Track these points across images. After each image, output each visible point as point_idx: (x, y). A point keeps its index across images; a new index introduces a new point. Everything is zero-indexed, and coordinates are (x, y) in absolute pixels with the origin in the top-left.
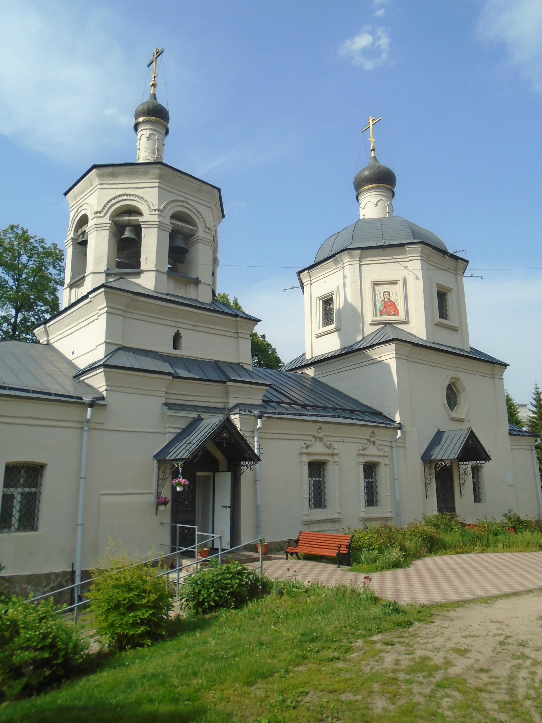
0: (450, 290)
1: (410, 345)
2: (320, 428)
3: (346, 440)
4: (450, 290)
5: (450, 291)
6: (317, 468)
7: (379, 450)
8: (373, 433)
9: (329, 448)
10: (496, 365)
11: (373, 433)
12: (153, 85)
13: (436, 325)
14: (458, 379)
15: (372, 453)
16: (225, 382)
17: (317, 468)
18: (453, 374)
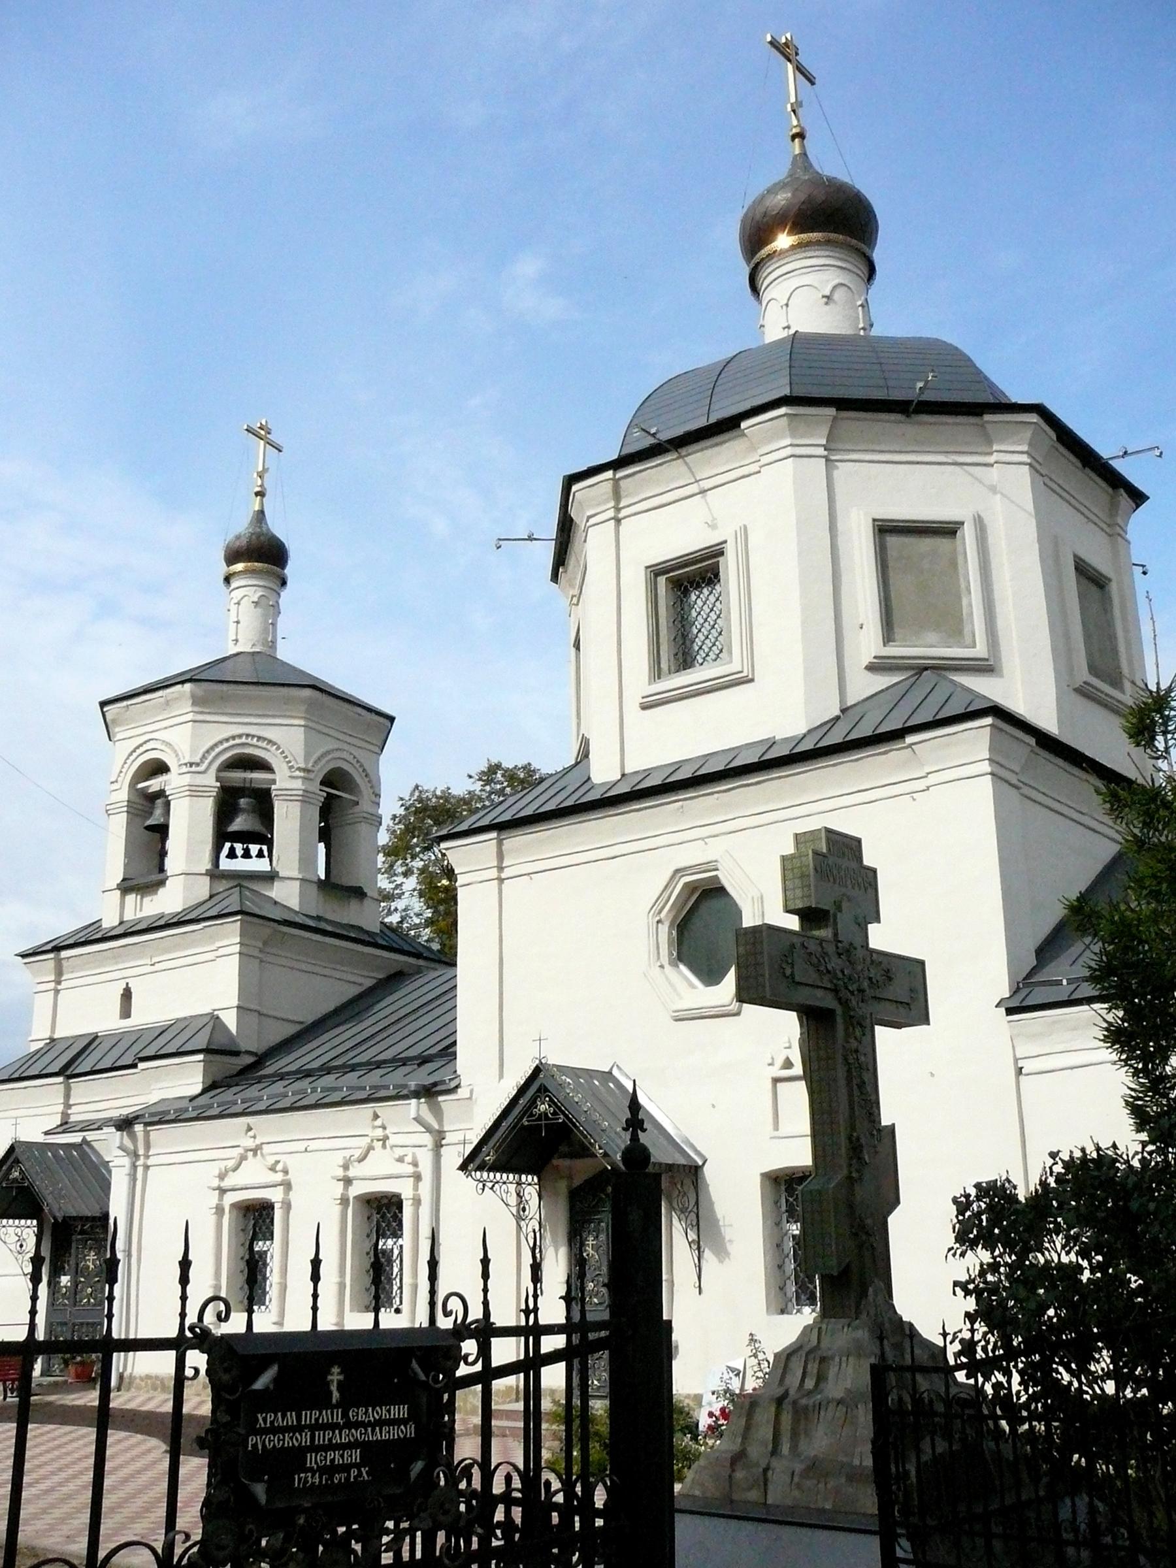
0: (717, 552)
2: (250, 1129)
3: (313, 1145)
4: (717, 552)
5: (722, 553)
6: (256, 1218)
7: (401, 1160)
8: (376, 1116)
9: (273, 1169)
10: (909, 739)
12: (260, 494)
13: (645, 707)
14: (712, 866)
15: (380, 1174)
16: (134, 1066)
18: (691, 855)
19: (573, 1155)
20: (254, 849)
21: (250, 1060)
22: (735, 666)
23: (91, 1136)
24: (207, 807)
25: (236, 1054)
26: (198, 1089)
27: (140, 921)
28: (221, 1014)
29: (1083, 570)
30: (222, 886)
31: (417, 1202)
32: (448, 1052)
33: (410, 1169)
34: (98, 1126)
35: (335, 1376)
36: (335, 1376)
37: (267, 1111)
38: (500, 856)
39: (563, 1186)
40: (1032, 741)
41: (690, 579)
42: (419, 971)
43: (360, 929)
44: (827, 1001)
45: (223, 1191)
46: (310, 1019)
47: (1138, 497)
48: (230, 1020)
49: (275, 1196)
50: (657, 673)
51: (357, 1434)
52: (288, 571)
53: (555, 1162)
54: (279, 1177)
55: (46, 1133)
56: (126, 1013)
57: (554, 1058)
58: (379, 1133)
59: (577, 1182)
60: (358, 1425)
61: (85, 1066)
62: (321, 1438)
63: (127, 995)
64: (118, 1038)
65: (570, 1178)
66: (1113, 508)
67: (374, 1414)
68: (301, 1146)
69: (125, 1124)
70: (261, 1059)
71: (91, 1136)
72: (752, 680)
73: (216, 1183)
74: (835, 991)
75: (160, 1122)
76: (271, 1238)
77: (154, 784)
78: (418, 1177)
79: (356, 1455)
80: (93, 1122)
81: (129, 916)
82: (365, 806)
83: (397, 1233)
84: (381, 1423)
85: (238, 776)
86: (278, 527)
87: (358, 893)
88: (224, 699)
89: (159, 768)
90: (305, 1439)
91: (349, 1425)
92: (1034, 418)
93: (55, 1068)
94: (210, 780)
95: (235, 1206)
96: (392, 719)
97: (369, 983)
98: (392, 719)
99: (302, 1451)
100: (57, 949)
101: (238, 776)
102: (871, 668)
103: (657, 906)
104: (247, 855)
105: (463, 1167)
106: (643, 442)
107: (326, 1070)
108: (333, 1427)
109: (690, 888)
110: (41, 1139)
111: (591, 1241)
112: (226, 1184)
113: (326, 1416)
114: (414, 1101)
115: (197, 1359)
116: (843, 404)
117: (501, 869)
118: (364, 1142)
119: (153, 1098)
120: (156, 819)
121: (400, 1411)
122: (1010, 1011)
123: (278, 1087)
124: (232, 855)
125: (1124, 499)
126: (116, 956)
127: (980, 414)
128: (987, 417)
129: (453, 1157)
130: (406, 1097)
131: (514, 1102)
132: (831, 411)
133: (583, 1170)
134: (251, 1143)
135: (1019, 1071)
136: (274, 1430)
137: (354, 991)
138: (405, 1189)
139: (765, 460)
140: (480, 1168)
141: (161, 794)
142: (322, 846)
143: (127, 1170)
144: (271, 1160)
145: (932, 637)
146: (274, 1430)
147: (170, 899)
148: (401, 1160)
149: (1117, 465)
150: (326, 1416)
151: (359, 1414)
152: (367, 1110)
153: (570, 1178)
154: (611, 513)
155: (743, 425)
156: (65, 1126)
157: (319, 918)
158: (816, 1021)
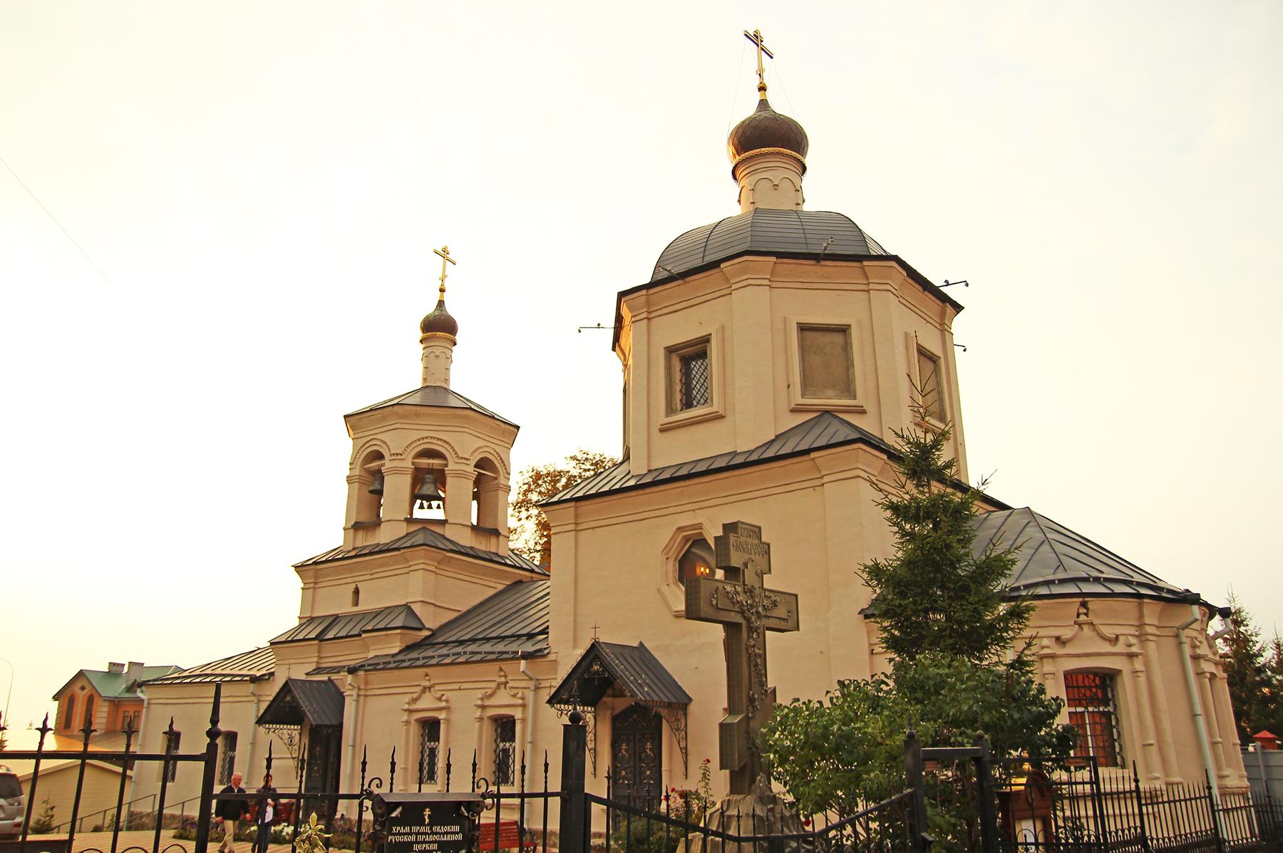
0: (706, 340)
1: (572, 504)
3: (464, 686)
4: (706, 340)
6: (431, 728)
7: (514, 696)
9: (440, 699)
10: (813, 455)
11: (501, 670)
13: (662, 431)
14: (699, 526)
15: (503, 702)
17: (431, 728)
19: (614, 696)
20: (435, 504)
21: (428, 633)
22: (714, 409)
23: (334, 677)
24: (407, 481)
25: (420, 629)
26: (396, 650)
27: (365, 547)
28: (412, 606)
29: (922, 352)
30: (414, 528)
31: (524, 720)
32: (545, 631)
33: (520, 702)
34: (337, 670)
35: (427, 812)
36: (427, 812)
37: (437, 665)
38: (577, 516)
39: (608, 714)
40: (885, 457)
41: (691, 355)
42: (533, 581)
43: (497, 554)
44: (738, 619)
45: (410, 711)
46: (464, 609)
47: (958, 308)
48: (417, 609)
49: (442, 716)
50: (670, 410)
51: (436, 837)
52: (458, 337)
53: (604, 699)
54: (443, 704)
55: (307, 674)
56: (356, 603)
57: (603, 639)
58: (503, 679)
59: (617, 711)
60: (436, 833)
61: (330, 635)
62: (420, 838)
63: (357, 592)
64: (350, 617)
65: (613, 709)
66: (943, 314)
67: (444, 829)
68: (456, 686)
69: (352, 671)
70: (434, 633)
71: (334, 677)
72: (723, 417)
73: (406, 707)
74: (742, 613)
75: (374, 670)
76: (438, 740)
77: (374, 464)
78: (524, 706)
79: (436, 846)
80: (334, 668)
81: (359, 544)
82: (502, 481)
83: (513, 739)
84: (447, 833)
85: (425, 462)
86: (452, 310)
87: (496, 533)
88: (417, 415)
89: (380, 456)
90: (413, 838)
91: (433, 833)
92: (894, 264)
93: (313, 635)
94: (408, 464)
95: (417, 720)
96: (518, 428)
97: (501, 587)
98: (518, 428)
99: (411, 844)
100: (315, 563)
101: (425, 462)
102: (793, 411)
103: (666, 550)
104: (430, 507)
105: (549, 702)
106: (665, 274)
107: (473, 640)
108: (426, 834)
109: (687, 539)
110: (303, 677)
111: (624, 746)
112: (414, 707)
113: (423, 829)
114: (523, 662)
115: (368, 803)
116: (779, 255)
117: (576, 524)
118: (494, 685)
119: (371, 655)
120: (377, 486)
121: (457, 828)
122: (866, 617)
123: (444, 651)
124: (422, 507)
125: (949, 309)
126: (350, 569)
127: (861, 261)
128: (865, 263)
129: (545, 695)
130: (518, 659)
131: (579, 664)
132: (774, 259)
133: (621, 704)
134: (427, 684)
135: (872, 652)
136: (399, 834)
137: (492, 592)
138: (518, 714)
139: (734, 287)
140: (560, 702)
141: (379, 471)
142: (475, 504)
143: (355, 697)
144: (439, 694)
145: (830, 392)
146: (399, 834)
147: (384, 536)
148: (514, 696)
149: (944, 290)
150: (423, 829)
151: (436, 829)
152: (496, 666)
153: (613, 709)
154: (645, 315)
155: (722, 266)
156: (318, 670)
157: (472, 548)
158: (731, 628)
